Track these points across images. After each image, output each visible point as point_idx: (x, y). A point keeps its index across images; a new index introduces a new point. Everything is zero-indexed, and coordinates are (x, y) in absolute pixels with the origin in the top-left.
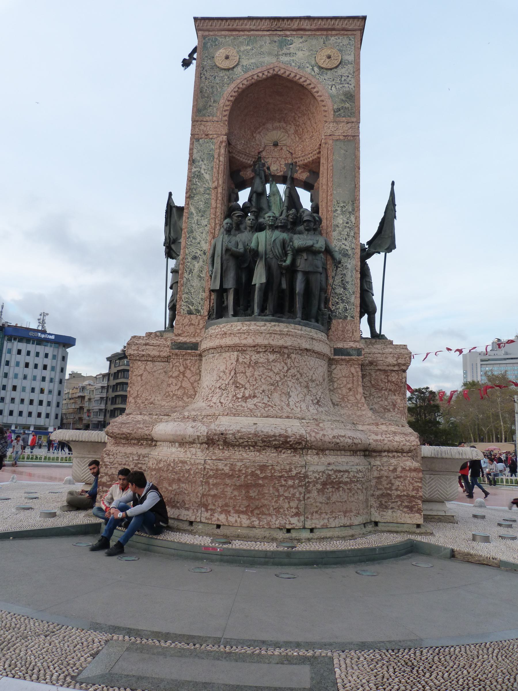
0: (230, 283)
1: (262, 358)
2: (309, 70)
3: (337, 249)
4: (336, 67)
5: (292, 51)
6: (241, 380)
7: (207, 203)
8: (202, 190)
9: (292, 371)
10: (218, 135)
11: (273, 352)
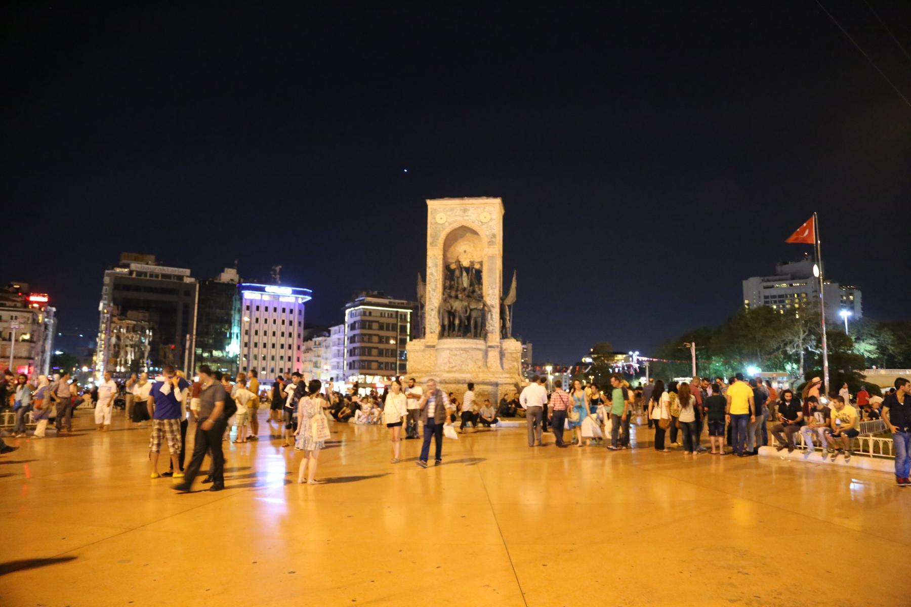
0: (446, 323)
1: (458, 353)
2: (477, 223)
3: (489, 305)
4: (489, 222)
5: (469, 214)
6: (451, 361)
7: (436, 286)
8: (433, 280)
9: (469, 357)
10: (439, 255)
11: (462, 350)
